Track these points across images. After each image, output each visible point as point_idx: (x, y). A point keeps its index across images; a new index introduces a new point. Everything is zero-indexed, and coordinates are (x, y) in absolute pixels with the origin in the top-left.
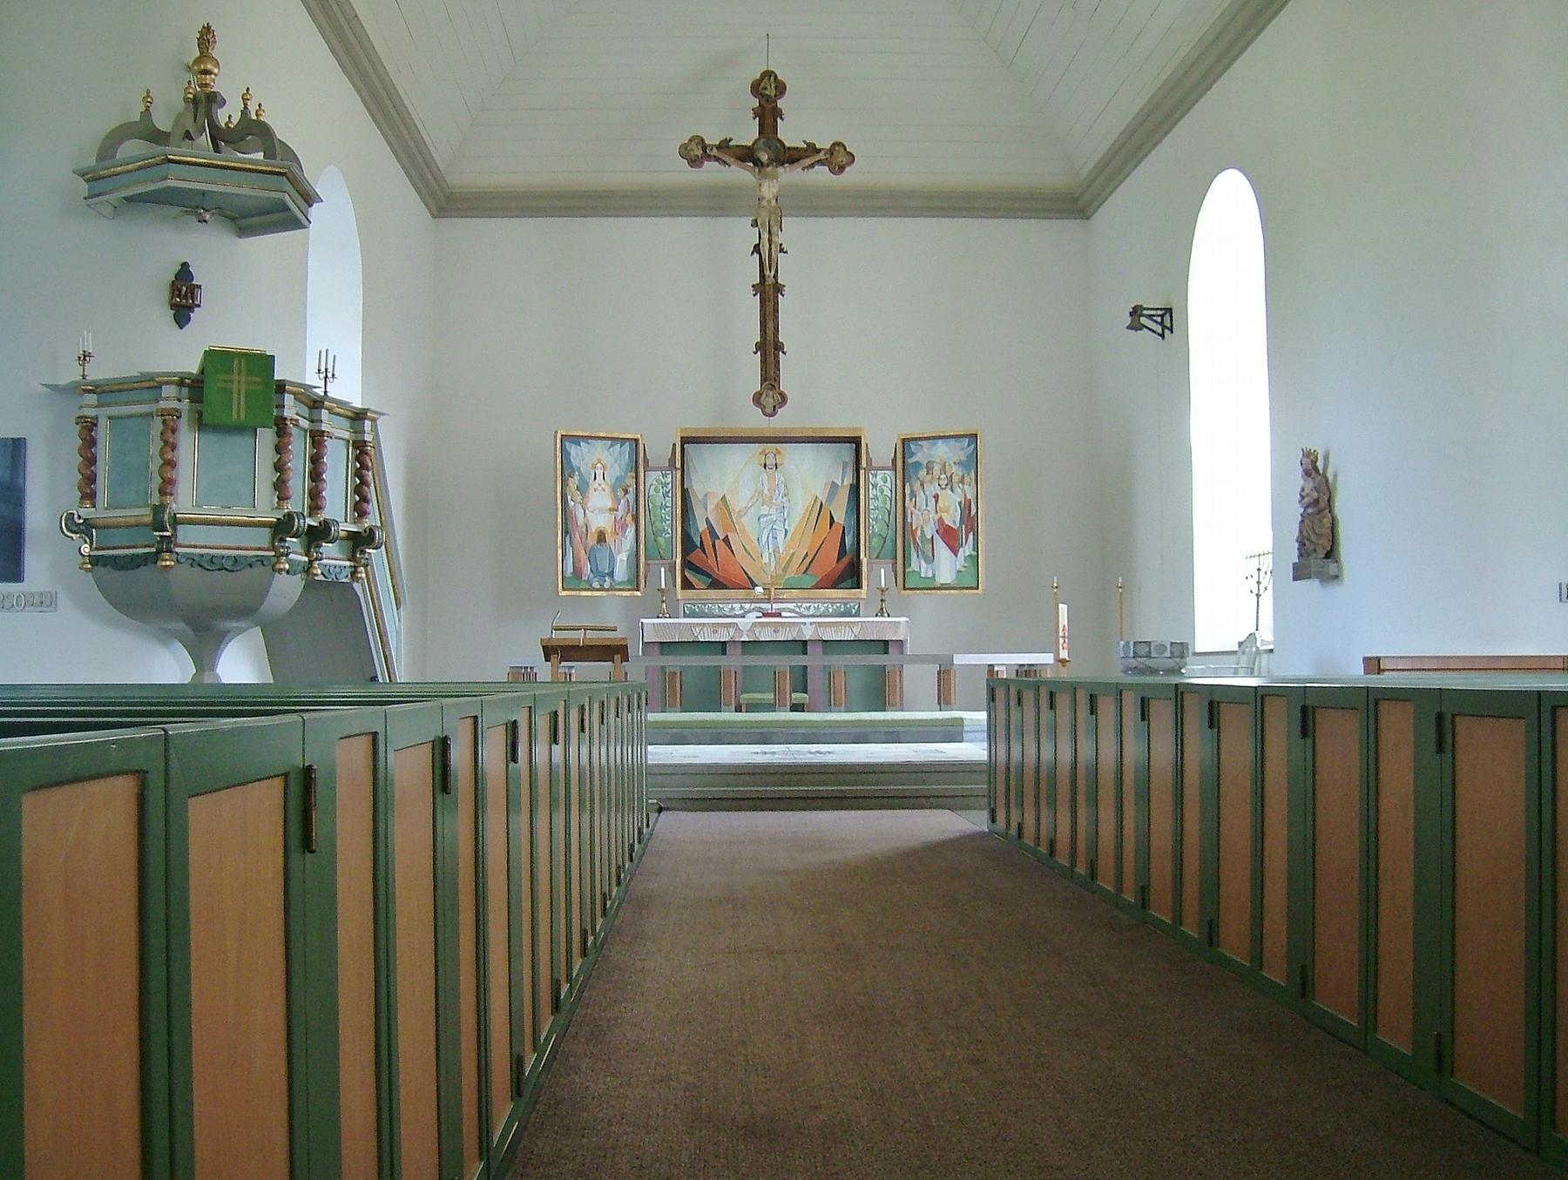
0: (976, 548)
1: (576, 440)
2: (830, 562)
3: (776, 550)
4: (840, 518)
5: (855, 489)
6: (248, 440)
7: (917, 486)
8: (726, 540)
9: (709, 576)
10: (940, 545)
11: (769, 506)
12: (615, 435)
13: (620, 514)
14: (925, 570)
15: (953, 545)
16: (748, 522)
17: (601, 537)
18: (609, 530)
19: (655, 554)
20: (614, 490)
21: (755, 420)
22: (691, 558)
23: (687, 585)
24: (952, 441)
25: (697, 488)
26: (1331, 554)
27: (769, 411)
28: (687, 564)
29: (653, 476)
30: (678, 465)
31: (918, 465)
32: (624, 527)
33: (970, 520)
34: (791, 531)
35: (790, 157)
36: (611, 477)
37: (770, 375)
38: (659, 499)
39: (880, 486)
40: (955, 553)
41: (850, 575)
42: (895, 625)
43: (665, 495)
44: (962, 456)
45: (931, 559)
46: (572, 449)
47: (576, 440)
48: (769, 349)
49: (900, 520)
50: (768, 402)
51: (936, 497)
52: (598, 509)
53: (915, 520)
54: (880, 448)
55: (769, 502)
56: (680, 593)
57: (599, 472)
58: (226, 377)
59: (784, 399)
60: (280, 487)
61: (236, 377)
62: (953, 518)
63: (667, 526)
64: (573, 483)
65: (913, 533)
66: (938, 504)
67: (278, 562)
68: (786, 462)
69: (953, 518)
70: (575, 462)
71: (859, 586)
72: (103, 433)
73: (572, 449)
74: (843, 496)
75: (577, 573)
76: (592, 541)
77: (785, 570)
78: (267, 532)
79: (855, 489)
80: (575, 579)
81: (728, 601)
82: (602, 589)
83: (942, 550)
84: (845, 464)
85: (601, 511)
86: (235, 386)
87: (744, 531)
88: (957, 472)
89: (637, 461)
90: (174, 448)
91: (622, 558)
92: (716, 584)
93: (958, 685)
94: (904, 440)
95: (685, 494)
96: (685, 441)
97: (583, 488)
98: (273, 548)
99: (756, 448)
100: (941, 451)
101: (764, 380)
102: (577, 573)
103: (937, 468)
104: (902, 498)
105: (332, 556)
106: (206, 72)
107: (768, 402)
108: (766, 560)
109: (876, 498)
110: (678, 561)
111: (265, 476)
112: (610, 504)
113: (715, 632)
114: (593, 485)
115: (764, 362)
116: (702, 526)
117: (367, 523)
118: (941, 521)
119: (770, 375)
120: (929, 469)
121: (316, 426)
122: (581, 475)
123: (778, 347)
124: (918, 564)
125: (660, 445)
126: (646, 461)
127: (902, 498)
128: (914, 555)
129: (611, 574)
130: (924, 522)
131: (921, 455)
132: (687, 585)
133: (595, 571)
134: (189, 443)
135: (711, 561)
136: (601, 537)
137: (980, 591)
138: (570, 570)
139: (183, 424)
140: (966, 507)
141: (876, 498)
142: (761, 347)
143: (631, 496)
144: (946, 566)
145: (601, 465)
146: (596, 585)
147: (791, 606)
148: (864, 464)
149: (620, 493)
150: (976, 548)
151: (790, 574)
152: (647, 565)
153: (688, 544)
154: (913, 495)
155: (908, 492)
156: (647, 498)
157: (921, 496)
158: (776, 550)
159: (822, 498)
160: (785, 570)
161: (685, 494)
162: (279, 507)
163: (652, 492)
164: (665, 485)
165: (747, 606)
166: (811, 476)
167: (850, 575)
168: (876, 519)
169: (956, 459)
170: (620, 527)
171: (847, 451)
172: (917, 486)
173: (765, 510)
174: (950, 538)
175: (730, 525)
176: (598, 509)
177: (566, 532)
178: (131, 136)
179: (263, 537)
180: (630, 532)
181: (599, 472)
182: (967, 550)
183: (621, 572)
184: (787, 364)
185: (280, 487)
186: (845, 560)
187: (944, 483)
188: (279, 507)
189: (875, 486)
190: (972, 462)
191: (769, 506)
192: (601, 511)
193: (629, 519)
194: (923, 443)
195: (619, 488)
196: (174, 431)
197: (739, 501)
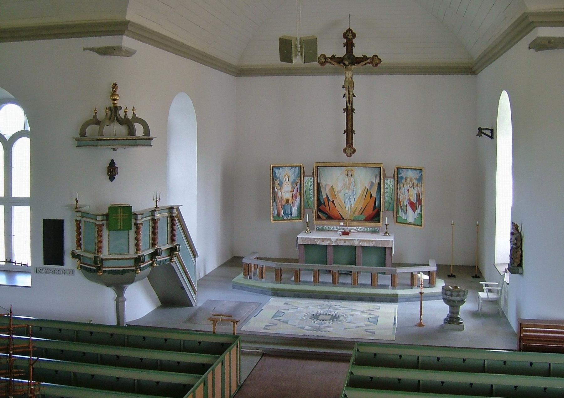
0: (421, 211)
1: (278, 168)
2: (370, 211)
3: (351, 206)
4: (374, 195)
5: (380, 184)
6: (127, 231)
7: (402, 185)
8: (333, 202)
9: (326, 214)
10: (409, 207)
11: (349, 190)
13: (294, 193)
14: (404, 217)
15: (414, 208)
16: (341, 195)
17: (287, 201)
18: (290, 199)
19: (307, 206)
20: (292, 184)
22: (320, 207)
23: (319, 218)
24: (414, 171)
25: (323, 183)
26: (520, 265)
28: (319, 210)
29: (307, 179)
31: (402, 178)
32: (296, 197)
33: (419, 201)
34: (356, 198)
35: (358, 61)
36: (291, 180)
37: (350, 142)
38: (309, 187)
39: (389, 184)
40: (414, 212)
41: (375, 217)
42: (389, 240)
45: (406, 213)
46: (277, 171)
48: (349, 132)
49: (395, 198)
50: (349, 151)
51: (408, 190)
52: (286, 191)
53: (401, 198)
55: (349, 188)
56: (315, 222)
57: (287, 179)
58: (115, 215)
59: (354, 151)
60: (137, 245)
61: (119, 215)
62: (414, 199)
64: (277, 183)
65: (400, 203)
66: (408, 193)
67: (137, 270)
69: (414, 199)
70: (278, 175)
71: (379, 221)
72: (82, 225)
73: (277, 171)
74: (376, 187)
75: (278, 215)
76: (284, 203)
77: (354, 213)
78: (133, 261)
81: (331, 226)
82: (287, 220)
84: (376, 175)
85: (287, 192)
86: (119, 218)
88: (416, 182)
89: (301, 173)
90: (101, 236)
91: (295, 209)
92: (330, 217)
93: (399, 280)
94: (398, 168)
95: (318, 185)
97: (281, 184)
98: (135, 266)
100: (410, 174)
102: (278, 215)
103: (408, 180)
104: (397, 190)
105: (163, 257)
106: (115, 100)
107: (349, 151)
108: (347, 209)
109: (387, 188)
111: (132, 242)
112: (290, 189)
113: (323, 241)
114: (284, 183)
115: (347, 137)
116: (324, 196)
117: (175, 244)
118: (409, 199)
119: (350, 142)
120: (406, 180)
121: (153, 217)
122: (280, 179)
123: (353, 132)
124: (401, 214)
126: (304, 173)
127: (397, 190)
128: (400, 210)
129: (291, 214)
130: (404, 199)
131: (403, 174)
132: (319, 218)
133: (285, 214)
134: (106, 233)
135: (327, 209)
136: (287, 201)
138: (276, 213)
139: (104, 227)
140: (418, 195)
142: (346, 131)
143: (298, 186)
144: (411, 216)
146: (285, 218)
149: (294, 185)
150: (421, 211)
151: (356, 214)
152: (304, 210)
153: (319, 203)
154: (400, 188)
155: (398, 187)
157: (403, 189)
159: (368, 187)
160: (354, 213)
161: (318, 185)
162: (136, 253)
163: (306, 184)
166: (363, 179)
167: (375, 217)
168: (387, 196)
169: (415, 177)
170: (295, 197)
172: (402, 185)
173: (347, 191)
174: (413, 206)
175: (334, 196)
176: (286, 191)
177: (274, 200)
178: (90, 124)
179: (132, 263)
180: (298, 199)
181: (287, 179)
182: (418, 211)
184: (356, 138)
185: (137, 245)
186: (376, 210)
188: (136, 253)
189: (387, 184)
191: (349, 190)
192: (287, 192)
193: (298, 194)
195: (294, 183)
196: (101, 231)
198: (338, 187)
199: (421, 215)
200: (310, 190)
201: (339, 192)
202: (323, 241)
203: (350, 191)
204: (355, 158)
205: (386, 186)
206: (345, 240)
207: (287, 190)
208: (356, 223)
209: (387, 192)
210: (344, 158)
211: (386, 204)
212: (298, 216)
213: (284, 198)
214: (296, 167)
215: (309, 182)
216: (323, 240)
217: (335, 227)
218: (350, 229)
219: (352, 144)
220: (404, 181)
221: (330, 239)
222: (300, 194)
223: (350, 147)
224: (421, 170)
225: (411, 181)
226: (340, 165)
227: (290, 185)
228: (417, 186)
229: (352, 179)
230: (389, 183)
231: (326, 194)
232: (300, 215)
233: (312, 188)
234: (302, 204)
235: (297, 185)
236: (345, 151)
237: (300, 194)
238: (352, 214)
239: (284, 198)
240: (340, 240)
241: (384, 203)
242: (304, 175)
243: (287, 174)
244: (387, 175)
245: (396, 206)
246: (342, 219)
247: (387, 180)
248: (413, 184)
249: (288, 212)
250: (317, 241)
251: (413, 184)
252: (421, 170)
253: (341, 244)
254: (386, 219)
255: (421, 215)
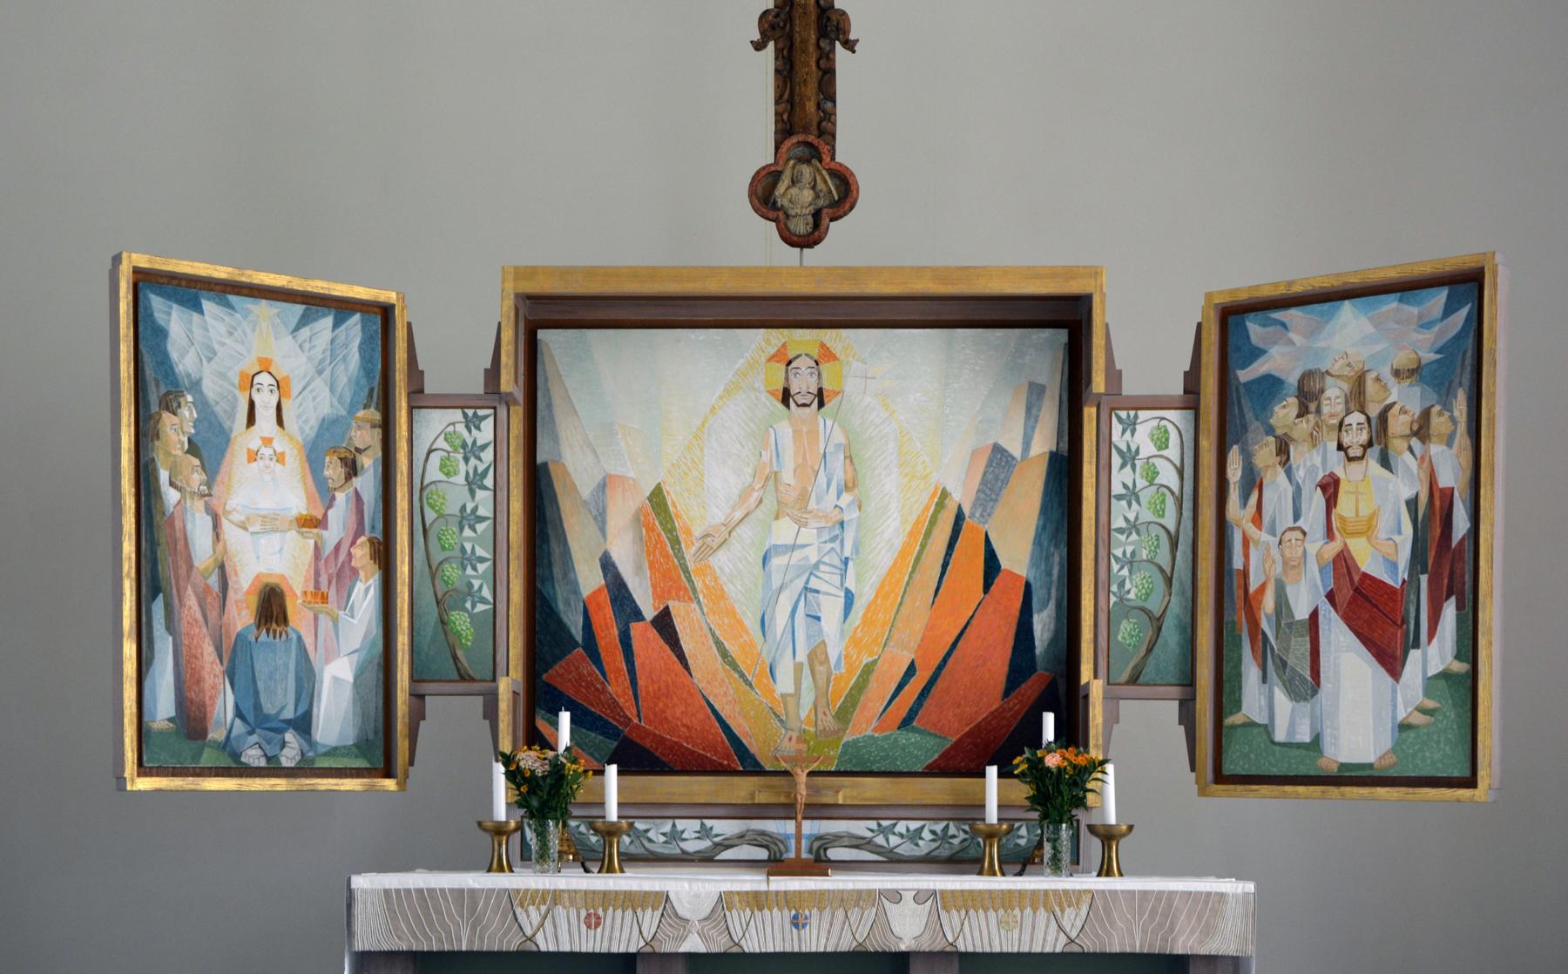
0: (1469, 646)
1: (189, 290)
3: (817, 655)
4: (1017, 557)
7: (1265, 454)
8: (664, 622)
12: (317, 286)
16: (731, 570)
17: (271, 606)
19: (445, 668)
20: (313, 458)
21: (753, 251)
22: (557, 675)
24: (1390, 304)
25: (576, 461)
27: (801, 226)
28: (541, 697)
29: (435, 425)
30: (510, 382)
31: (1270, 387)
32: (345, 575)
33: (1447, 556)
37: (805, 114)
38: (454, 496)
39: (1145, 457)
43: (474, 483)
44: (1423, 346)
46: (174, 319)
47: (189, 290)
50: (799, 198)
51: (1330, 488)
52: (261, 516)
53: (1260, 560)
54: (1147, 344)
55: (798, 507)
59: (843, 195)
62: (1385, 553)
63: (478, 577)
64: (176, 429)
65: (1250, 605)
68: (851, 386)
69: (1385, 553)
70: (185, 361)
73: (174, 319)
75: (191, 720)
76: (242, 616)
77: (844, 715)
79: (1065, 472)
80: (186, 740)
83: (1345, 655)
84: (1036, 392)
85: (271, 523)
87: (719, 595)
88: (1407, 400)
89: (390, 378)
96: (546, 313)
97: (209, 448)
99: (759, 342)
100: (1351, 337)
101: (786, 128)
102: (191, 720)
103: (1334, 396)
107: (799, 198)
108: (785, 684)
109: (1132, 495)
110: (509, 684)
113: (593, 922)
114: (244, 440)
115: (786, 74)
116: (590, 580)
118: (1343, 562)
119: (805, 114)
120: (1308, 397)
122: (202, 404)
124: (1263, 701)
125: (459, 335)
126: (415, 374)
128: (1251, 672)
129: (303, 724)
130: (1288, 563)
131: (1281, 353)
133: (253, 715)
135: (617, 688)
136: (271, 606)
137: (1480, 793)
138: (164, 707)
141: (1132, 495)
143: (368, 483)
144: (1361, 707)
145: (270, 378)
146: (253, 757)
147: (860, 828)
148: (1099, 384)
151: (865, 726)
152: (418, 697)
154: (1253, 482)
155: (1235, 473)
156: (420, 490)
157: (1277, 488)
158: (817, 655)
159: (962, 494)
160: (844, 715)
163: (434, 473)
164: (472, 451)
165: (725, 828)
166: (929, 429)
169: (1403, 359)
170: (333, 575)
171: (1042, 351)
172: (1265, 454)
173: (784, 532)
176: (261, 516)
177: (151, 585)
180: (365, 594)
181: (266, 402)
182: (1435, 654)
183: (336, 713)
186: (1031, 688)
187: (1356, 438)
189: (1130, 457)
190: (1462, 368)
191: (802, 519)
192: (271, 523)
193: (361, 553)
194: (1293, 315)
195: (328, 454)
197: (705, 504)
198: (710, 497)
199: (1463, 687)
200: (467, 518)
201: (712, 542)
202: (593, 922)
203: (808, 535)
204: (852, 251)
205: (1120, 478)
206: (798, 910)
207: (266, 504)
208: (872, 789)
209: (1133, 527)
210: (753, 251)
211: (1127, 631)
212: (362, 746)
213: (245, 581)
214: (343, 307)
215: (453, 454)
216: (594, 908)
217: (690, 827)
218: (824, 842)
219: (826, 131)
220: (1284, 413)
221: (662, 900)
222: (384, 555)
223: (812, 154)
224: (1468, 284)
225: (1357, 396)
226: (722, 314)
227: (294, 460)
228: (1421, 430)
229: (824, 422)
230: (1148, 450)
231: (607, 565)
232: (380, 750)
233: (484, 496)
234: (402, 640)
235: (352, 469)
236: (764, 195)
237: (384, 555)
238: (829, 722)
239: (245, 581)
240: (757, 901)
241: (1108, 620)
242: (419, 397)
243: (265, 366)
244: (1129, 388)
245: (1220, 630)
246: (737, 759)
247: (1131, 426)
248: (1380, 426)
249: (280, 701)
250: (530, 918)
251: (1380, 426)
252: (1468, 284)
253: (764, 935)
254: (1134, 750)
255: (1463, 687)
